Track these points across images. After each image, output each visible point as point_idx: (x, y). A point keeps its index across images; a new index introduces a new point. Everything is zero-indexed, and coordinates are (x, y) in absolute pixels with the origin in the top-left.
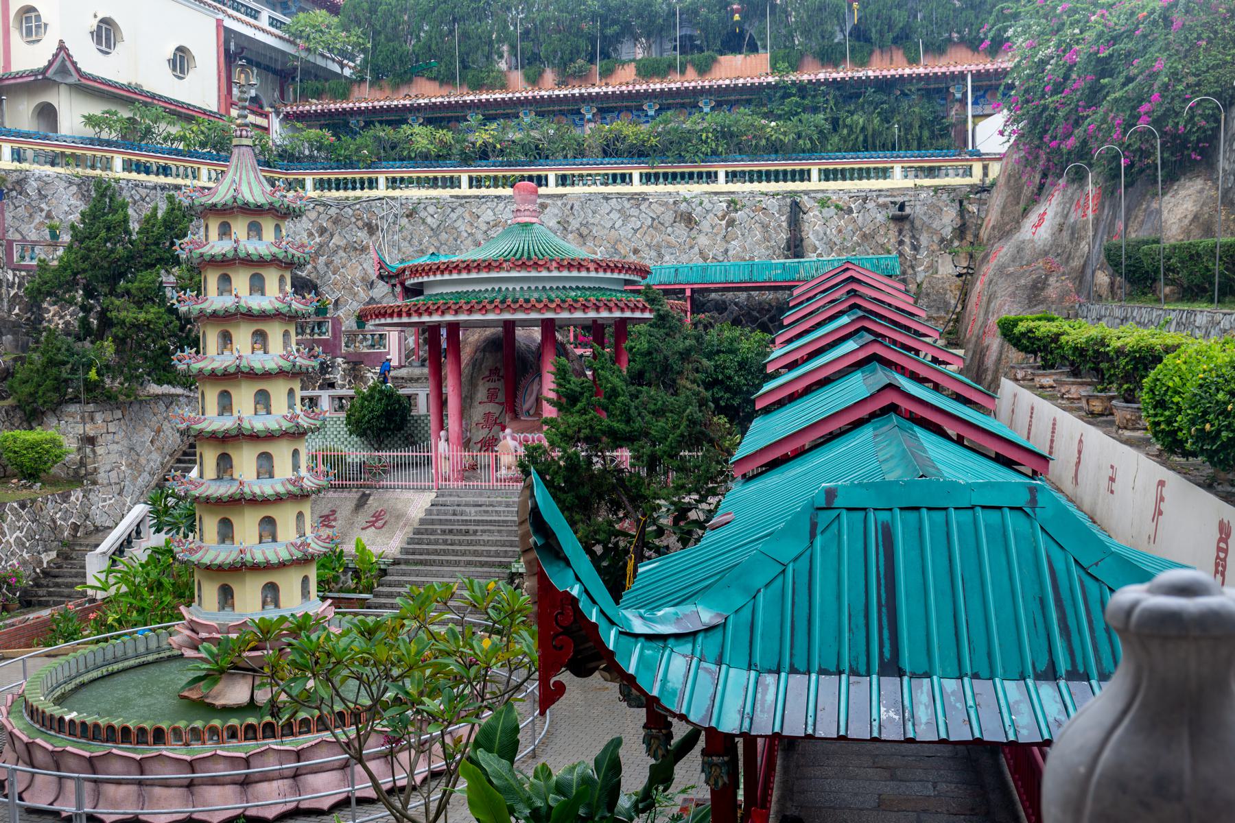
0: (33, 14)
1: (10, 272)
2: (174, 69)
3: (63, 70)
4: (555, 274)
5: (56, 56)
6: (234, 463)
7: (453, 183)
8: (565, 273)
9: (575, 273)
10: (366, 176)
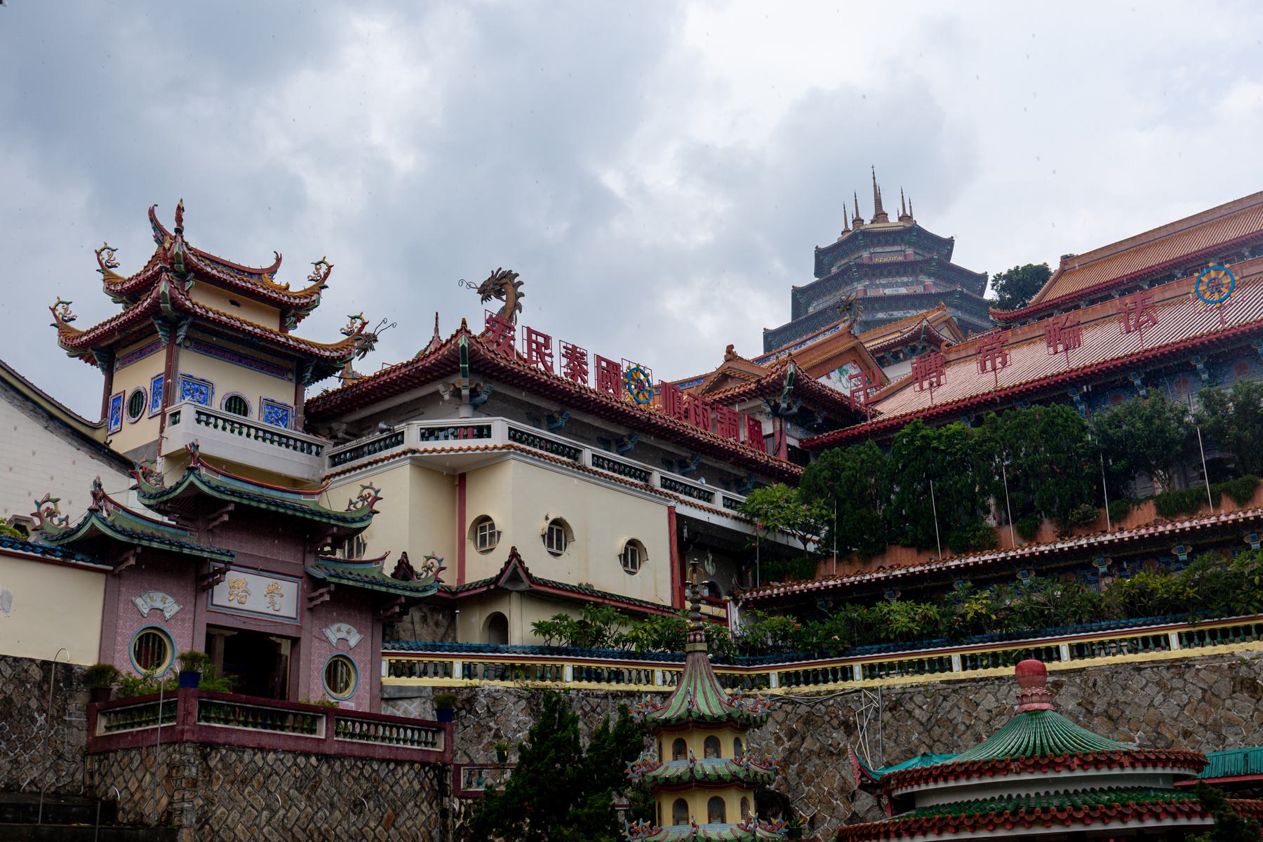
0: (487, 524)
1: (457, 800)
2: (626, 565)
3: (515, 578)
5: (508, 563)
7: (945, 665)
8: (1092, 772)
9: (1105, 771)
10: (838, 665)
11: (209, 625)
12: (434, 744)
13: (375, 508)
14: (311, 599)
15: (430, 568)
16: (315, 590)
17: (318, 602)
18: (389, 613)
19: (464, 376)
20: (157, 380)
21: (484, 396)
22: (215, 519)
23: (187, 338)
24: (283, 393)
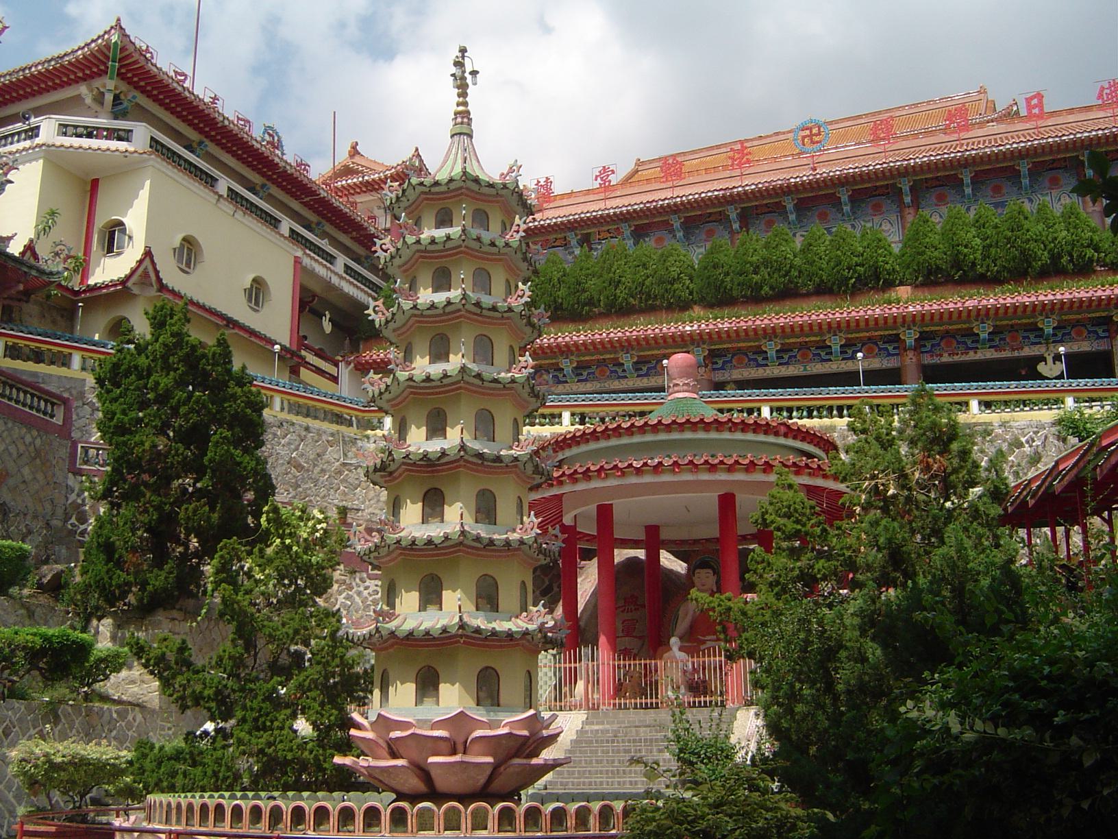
1: (70, 475)
2: (250, 300)
3: (145, 280)
5: (140, 262)
13: (9, 177)
18: (13, 292)
19: (111, 78)
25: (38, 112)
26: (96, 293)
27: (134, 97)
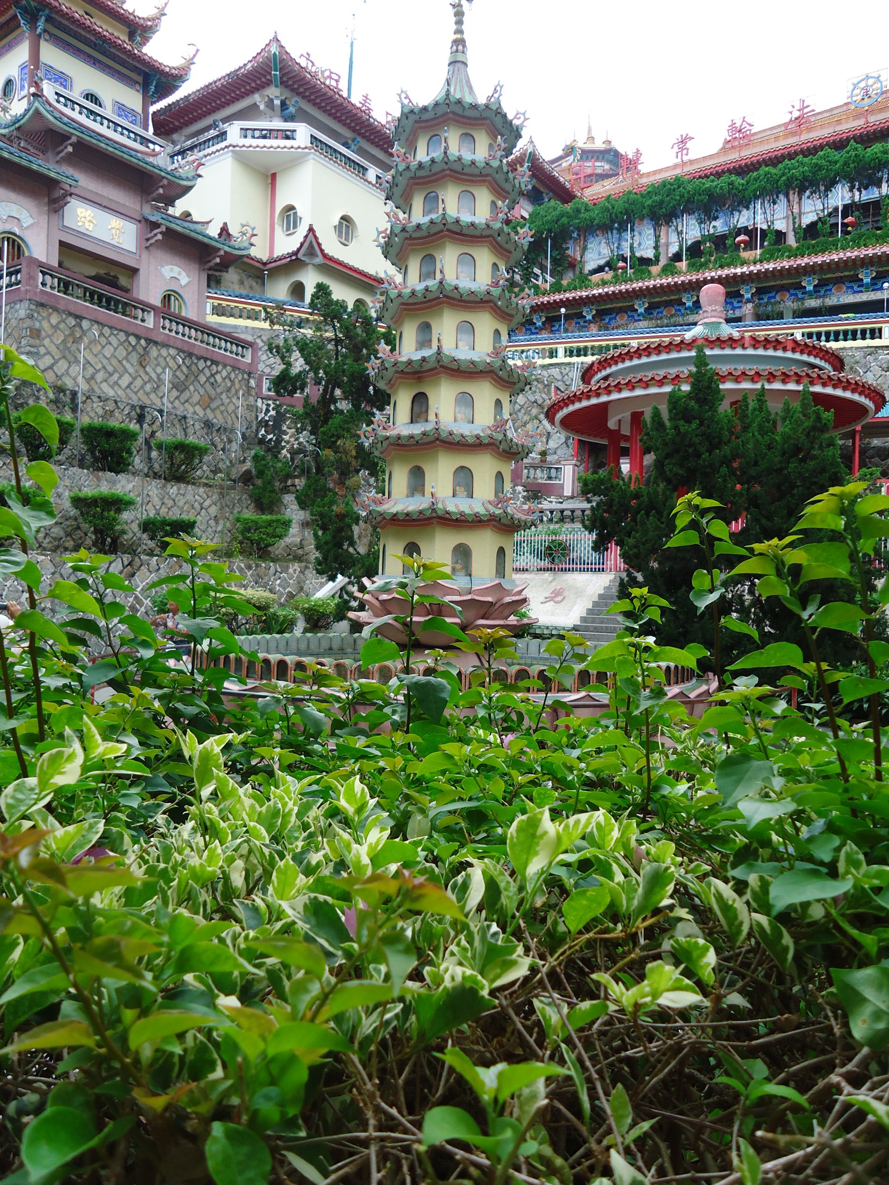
1: (259, 400)
3: (311, 253)
4: (750, 351)
5: (306, 237)
6: (431, 402)
8: (760, 352)
9: (770, 352)
11: (62, 244)
12: (243, 356)
13: (199, 172)
14: (148, 240)
15: (244, 234)
16: (151, 231)
17: (152, 241)
19: (276, 86)
20: (23, 68)
21: (292, 109)
22: (62, 151)
23: (45, 31)
24: (133, 99)
25: (225, 120)
26: (279, 263)
27: (297, 102)
